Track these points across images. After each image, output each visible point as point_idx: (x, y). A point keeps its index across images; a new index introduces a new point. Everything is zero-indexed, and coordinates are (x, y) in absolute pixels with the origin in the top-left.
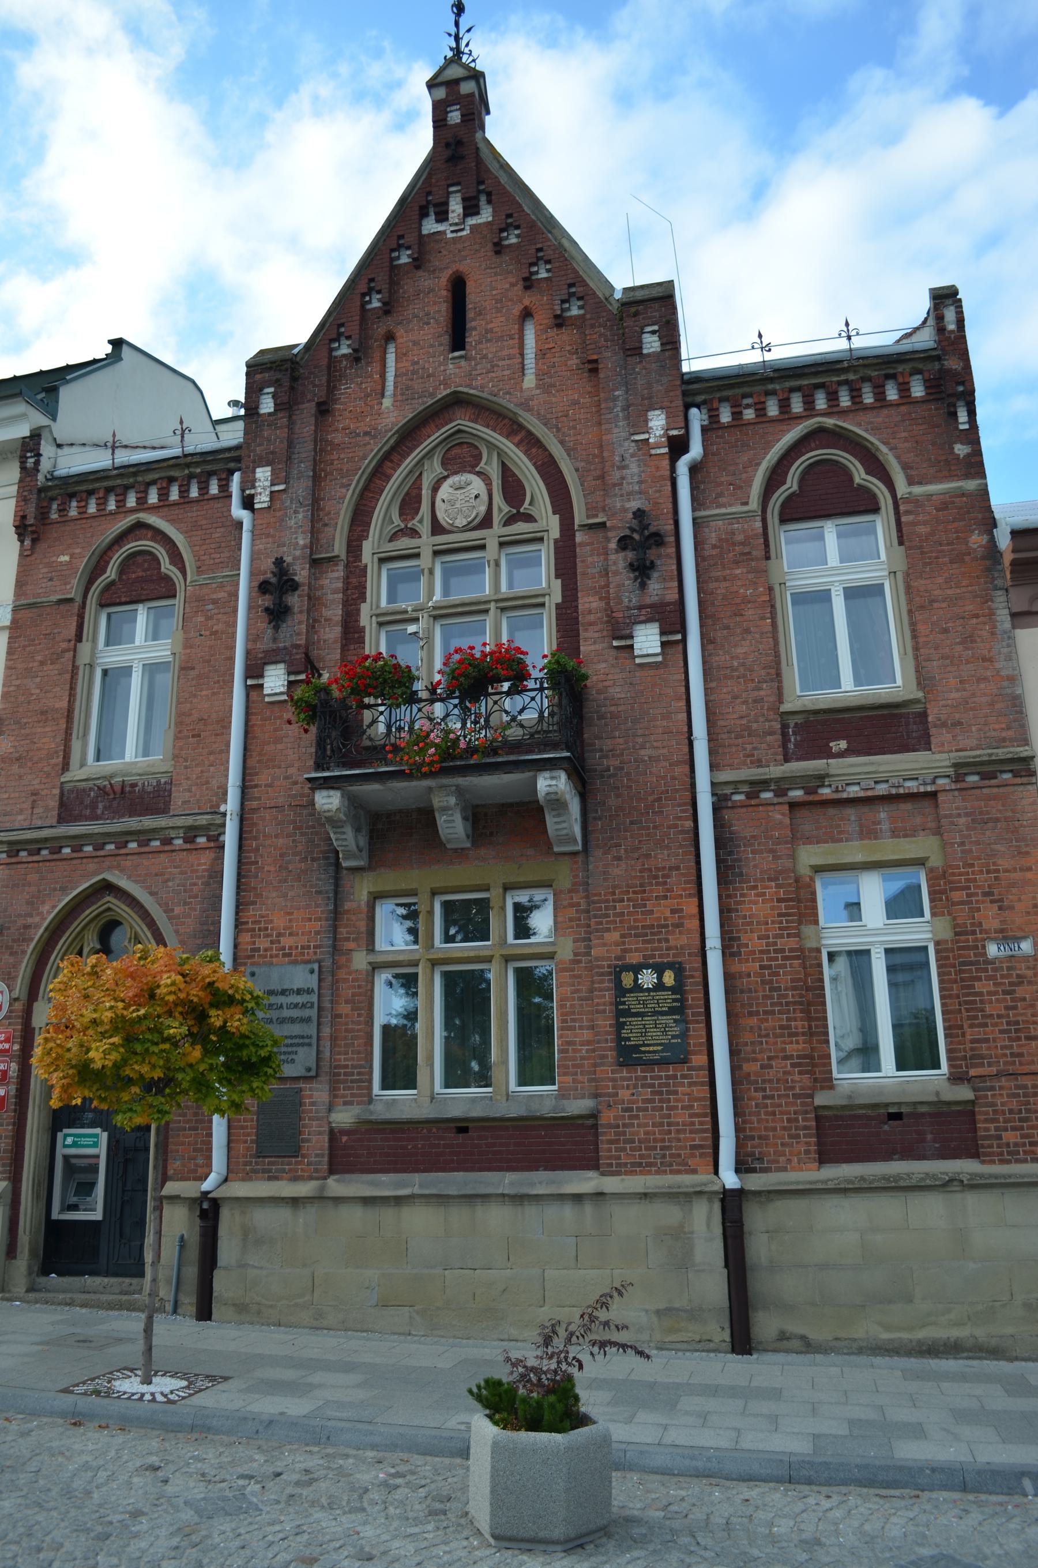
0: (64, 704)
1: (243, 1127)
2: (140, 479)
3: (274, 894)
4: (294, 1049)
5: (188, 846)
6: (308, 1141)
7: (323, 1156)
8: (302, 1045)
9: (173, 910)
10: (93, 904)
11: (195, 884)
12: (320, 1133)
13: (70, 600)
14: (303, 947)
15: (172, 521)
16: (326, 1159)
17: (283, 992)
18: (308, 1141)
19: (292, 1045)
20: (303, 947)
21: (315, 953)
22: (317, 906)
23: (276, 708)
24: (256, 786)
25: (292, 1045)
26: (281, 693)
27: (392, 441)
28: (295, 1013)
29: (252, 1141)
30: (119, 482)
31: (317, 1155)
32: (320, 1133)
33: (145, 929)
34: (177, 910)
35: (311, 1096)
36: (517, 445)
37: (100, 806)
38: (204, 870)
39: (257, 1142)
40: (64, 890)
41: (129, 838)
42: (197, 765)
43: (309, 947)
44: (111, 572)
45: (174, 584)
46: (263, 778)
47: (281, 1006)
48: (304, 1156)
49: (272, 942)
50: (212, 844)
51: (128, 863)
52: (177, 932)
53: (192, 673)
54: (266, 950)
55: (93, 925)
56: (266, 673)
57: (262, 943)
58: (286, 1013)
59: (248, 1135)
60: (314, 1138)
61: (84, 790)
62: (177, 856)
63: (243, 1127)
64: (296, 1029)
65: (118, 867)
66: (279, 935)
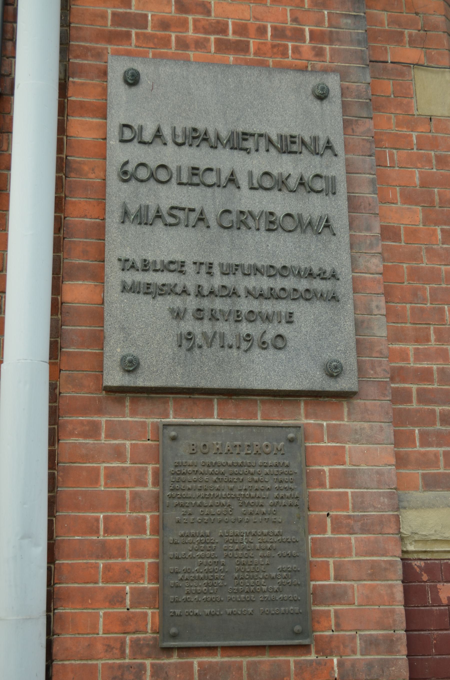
1: (104, 551)
4: (282, 307)
6: (337, 596)
7: (390, 644)
8: (308, 296)
12: (375, 572)
14: (279, 33)
16: (402, 656)
17: (239, 141)
18: (337, 596)
19: (273, 295)
20: (279, 33)
21: (320, 53)
25: (273, 295)
28: (279, 203)
29: (139, 598)
31: (371, 644)
32: (375, 572)
35: (337, 456)
39: (159, 599)
43: (298, 35)
47: (232, 179)
48: (325, 648)
54: (165, 25)
58: (249, 200)
59: (126, 575)
60: (357, 588)
63: (104, 551)
64: (283, 249)
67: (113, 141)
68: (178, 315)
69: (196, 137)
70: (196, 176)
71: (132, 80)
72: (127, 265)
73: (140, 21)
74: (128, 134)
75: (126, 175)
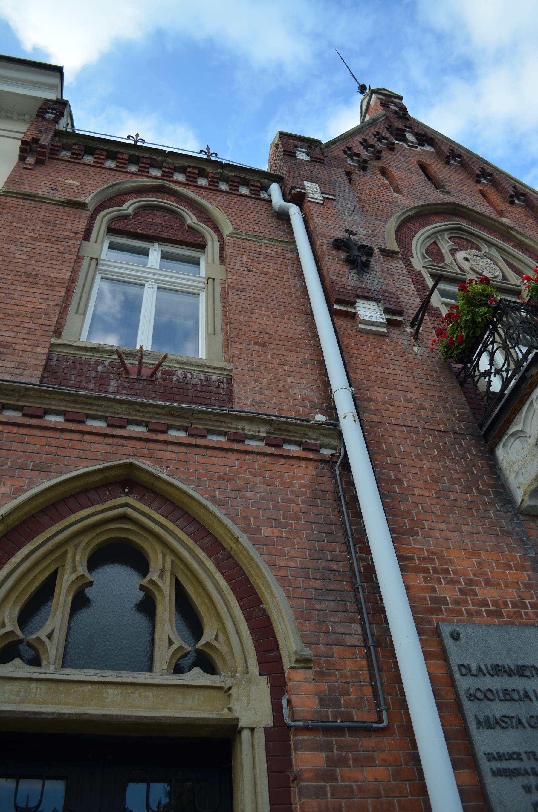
0: (66, 275)
2: (169, 160)
3: (443, 526)
5: (273, 450)
9: (259, 531)
10: (93, 503)
11: (292, 501)
13: (82, 206)
15: (202, 197)
22: (511, 550)
23: (373, 340)
24: (371, 400)
26: (380, 325)
27: (413, 212)
30: (147, 155)
33: (202, 555)
34: (266, 532)
36: (513, 246)
37: (114, 383)
38: (302, 486)
40: (42, 469)
41: (175, 422)
42: (267, 371)
43: (524, 606)
44: (129, 207)
45: (203, 237)
46: (379, 394)
47: (527, 696)
49: (462, 592)
50: (311, 455)
51: (171, 454)
52: (272, 565)
53: (244, 294)
54: (457, 602)
55: (85, 540)
56: (357, 304)
57: (451, 593)
61: (87, 363)
62: (257, 462)
65: (150, 457)
66: (469, 582)
67: (457, 676)
68: (527, 789)
69: (498, 670)
70: (507, 696)
71: (455, 636)
72: (491, 757)
73: (443, 601)
74: (464, 670)
75: (471, 697)
